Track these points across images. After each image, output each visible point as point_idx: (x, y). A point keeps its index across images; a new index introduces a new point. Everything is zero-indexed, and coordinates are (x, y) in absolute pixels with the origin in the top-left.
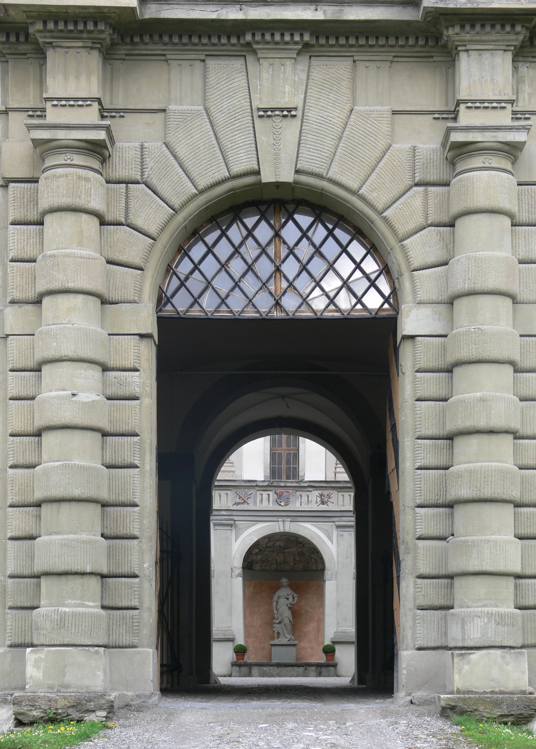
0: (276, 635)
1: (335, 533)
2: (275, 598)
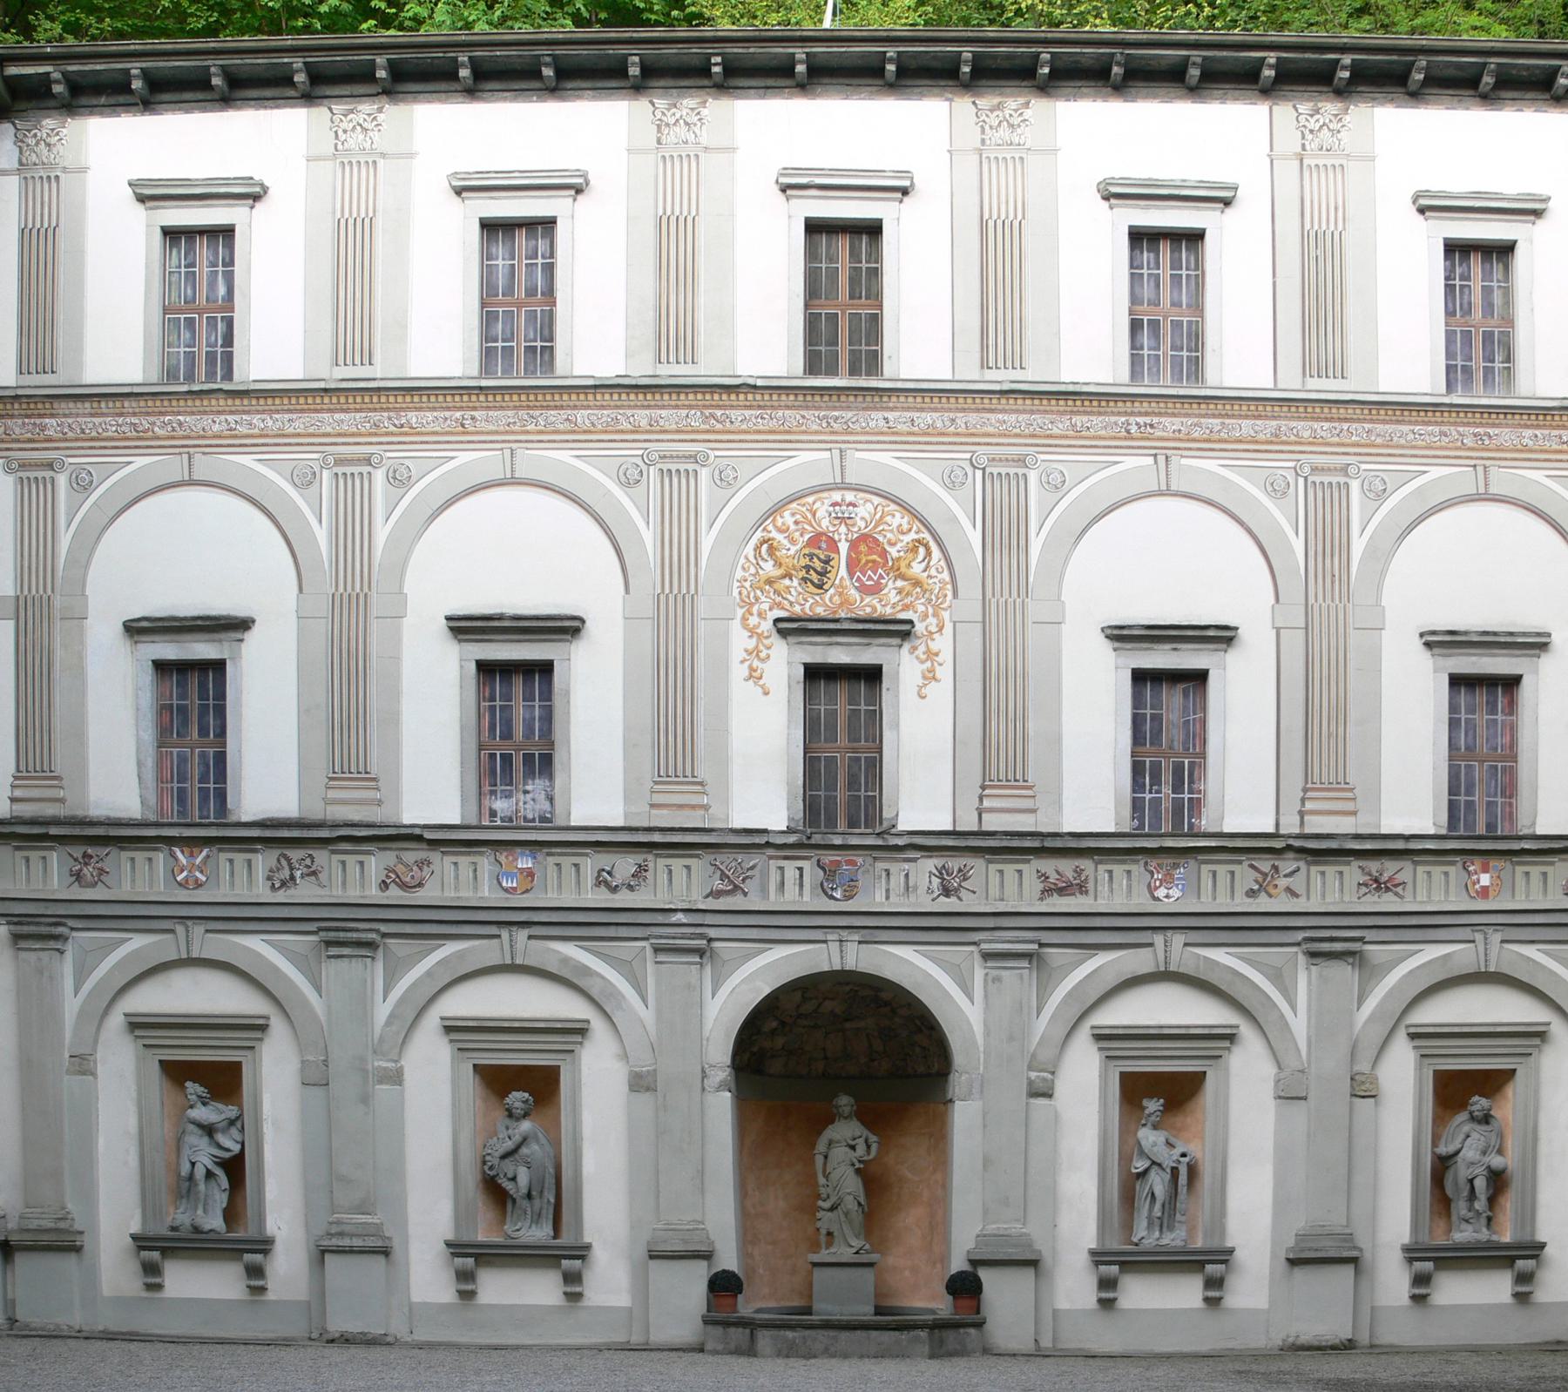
0: (823, 1239)
1: (979, 974)
2: (821, 1146)
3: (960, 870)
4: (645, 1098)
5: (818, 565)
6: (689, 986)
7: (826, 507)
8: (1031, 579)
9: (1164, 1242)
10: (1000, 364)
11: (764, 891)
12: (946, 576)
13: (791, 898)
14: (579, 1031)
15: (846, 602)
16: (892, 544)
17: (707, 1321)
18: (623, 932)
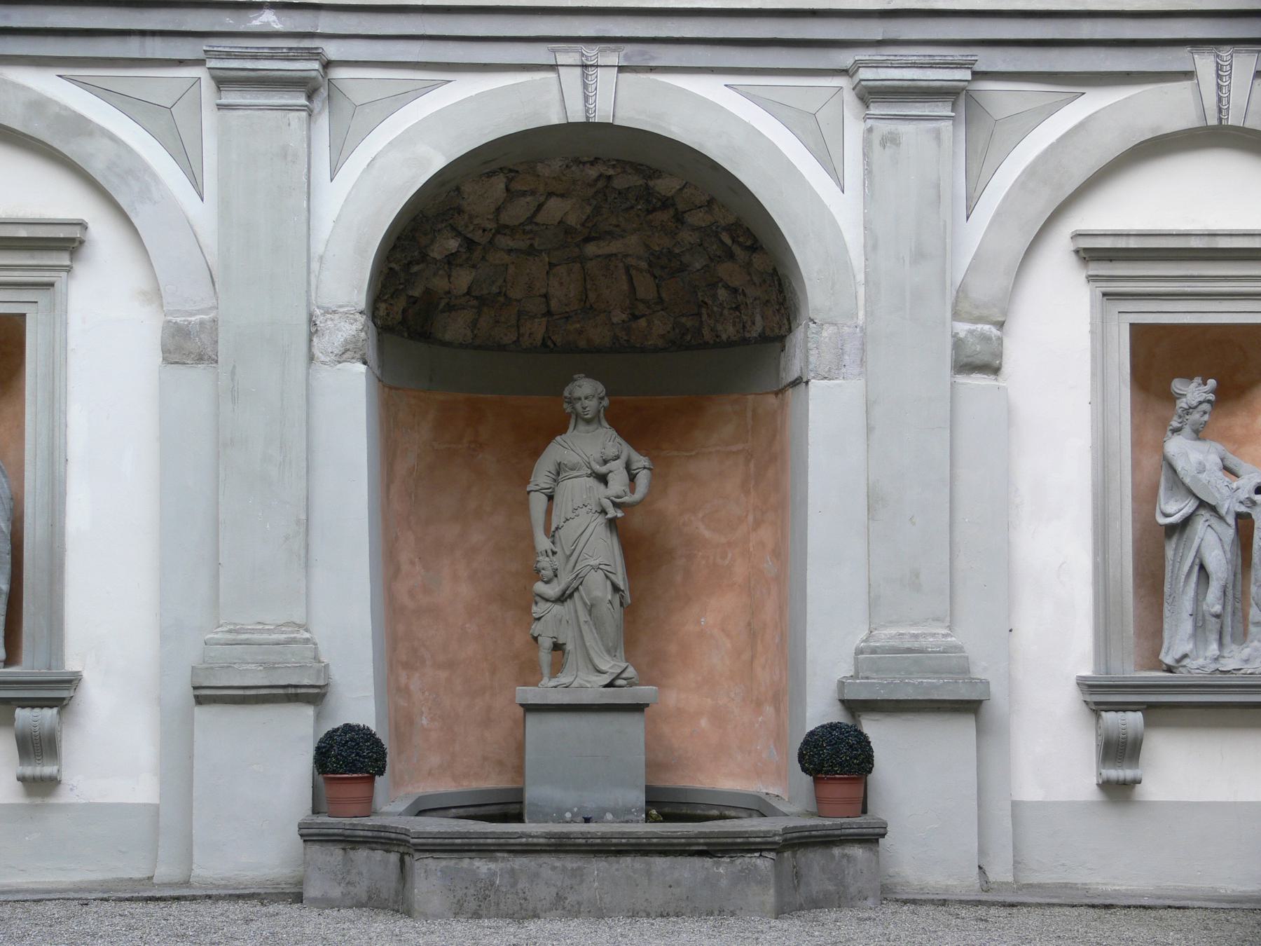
0: (545, 657)
1: (854, 130)
2: (541, 476)
4: (198, 375)
6: (284, 153)
9: (1229, 664)
14: (66, 244)
17: (310, 836)
18: (156, 48)
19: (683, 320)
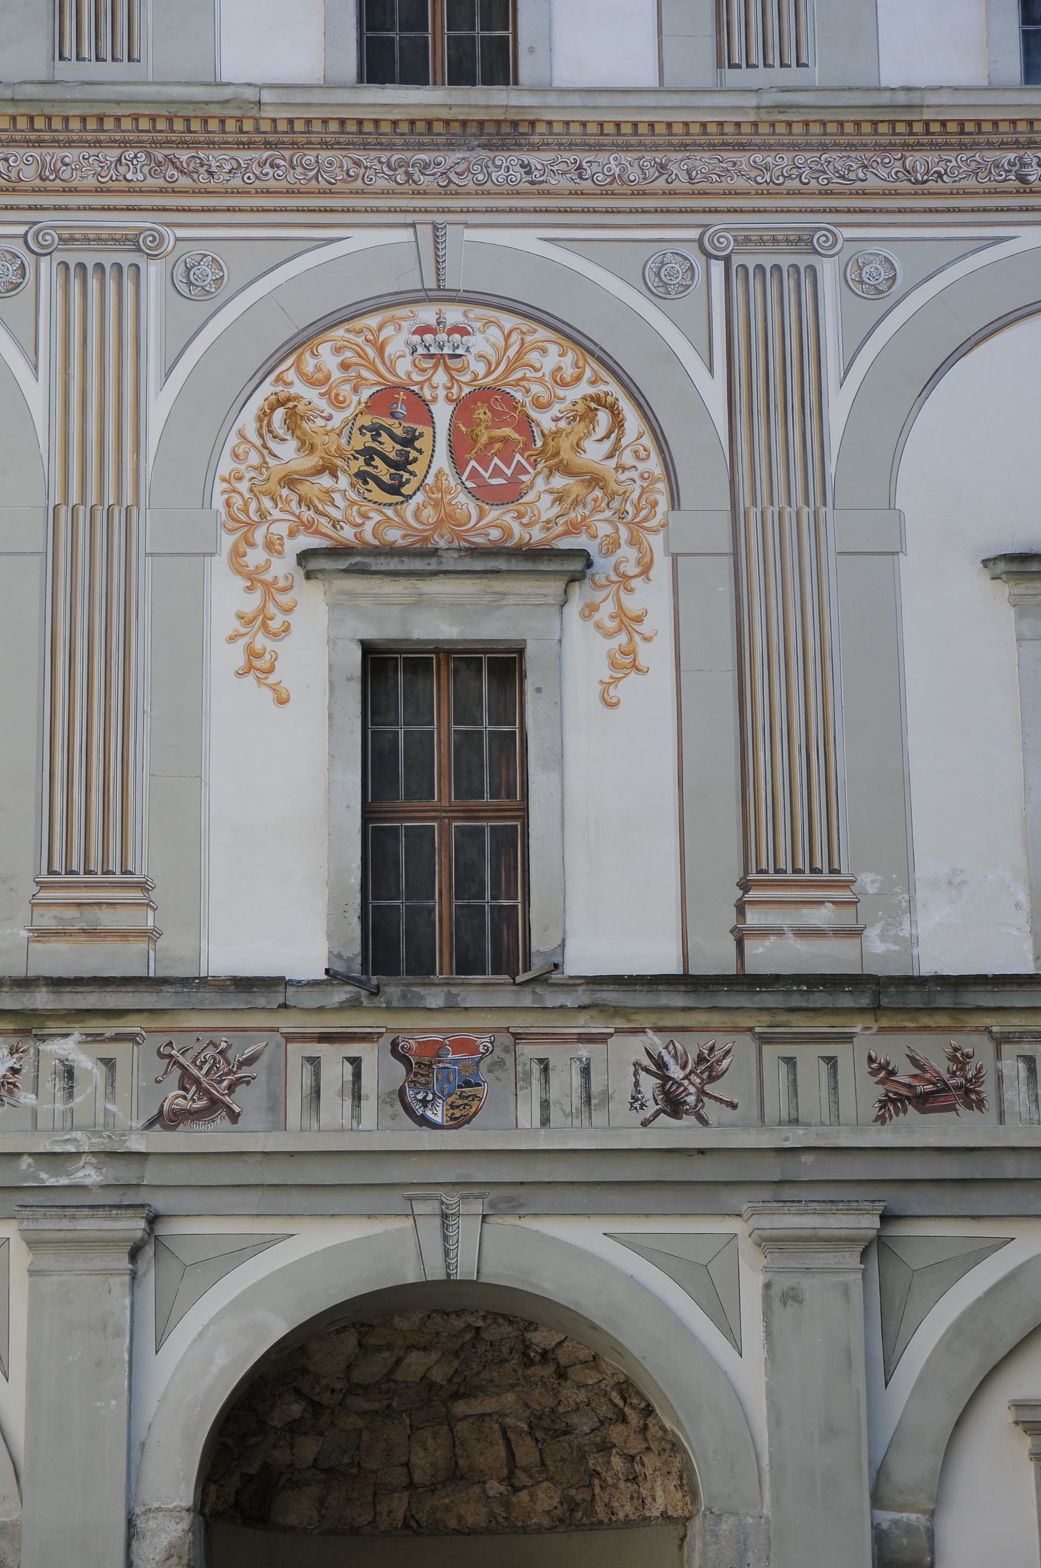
3: (701, 1059)
5: (389, 447)
7: (405, 335)
8: (831, 469)
10: (756, 57)
11: (276, 1107)
12: (654, 465)
13: (335, 1123)
15: (448, 519)
16: (541, 406)
19: (573, 1492)
